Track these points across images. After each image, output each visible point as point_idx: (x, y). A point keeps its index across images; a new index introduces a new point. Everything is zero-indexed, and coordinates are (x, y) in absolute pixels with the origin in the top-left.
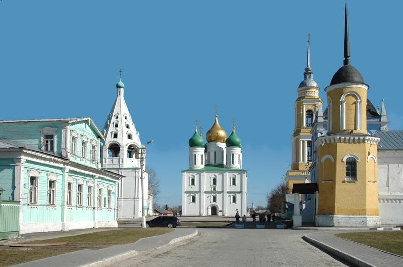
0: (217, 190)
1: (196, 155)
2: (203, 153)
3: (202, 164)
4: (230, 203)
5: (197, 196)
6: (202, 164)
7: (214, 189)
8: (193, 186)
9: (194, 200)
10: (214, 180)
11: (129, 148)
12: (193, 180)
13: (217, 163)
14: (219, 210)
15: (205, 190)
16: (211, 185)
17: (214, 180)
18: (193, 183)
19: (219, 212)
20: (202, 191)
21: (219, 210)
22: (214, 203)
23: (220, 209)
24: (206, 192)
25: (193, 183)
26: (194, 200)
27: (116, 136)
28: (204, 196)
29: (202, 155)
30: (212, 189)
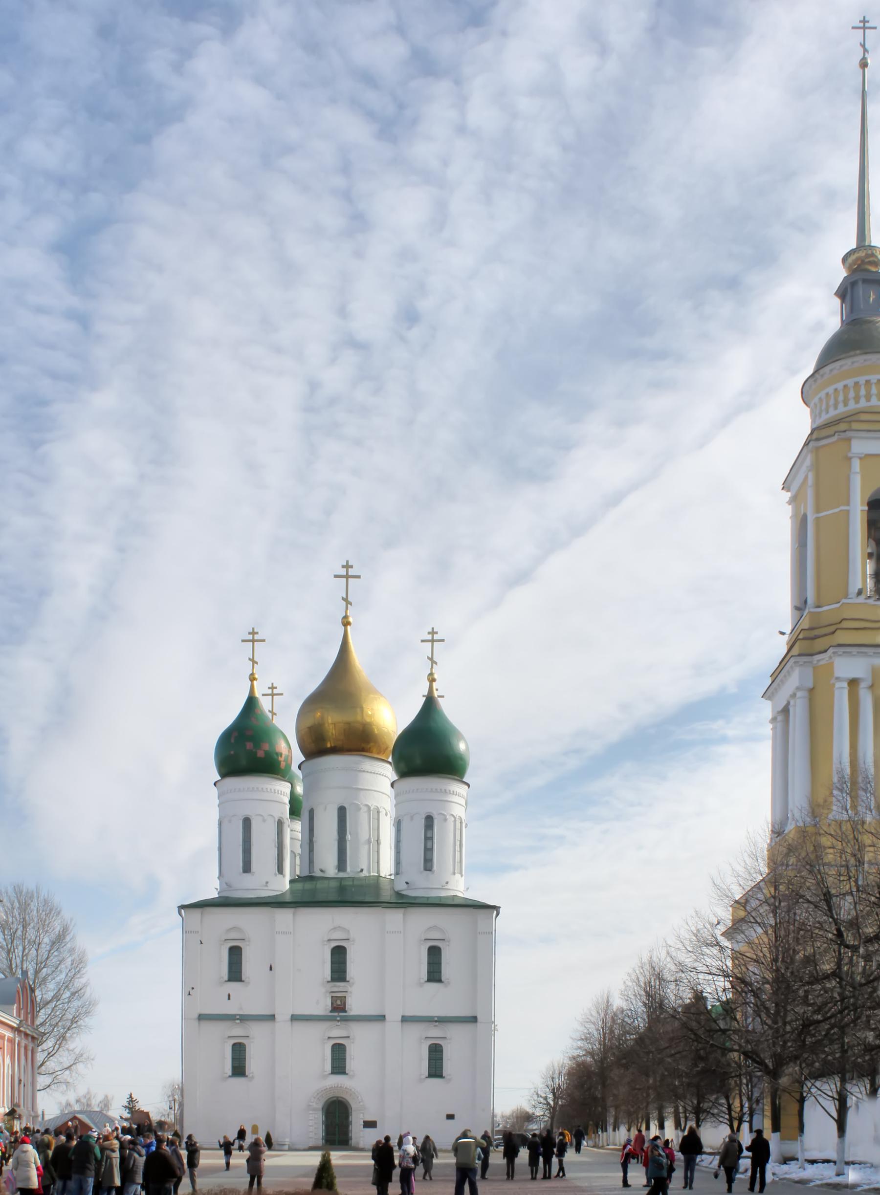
0: (355, 1006)
10: (339, 955)
17: (339, 955)
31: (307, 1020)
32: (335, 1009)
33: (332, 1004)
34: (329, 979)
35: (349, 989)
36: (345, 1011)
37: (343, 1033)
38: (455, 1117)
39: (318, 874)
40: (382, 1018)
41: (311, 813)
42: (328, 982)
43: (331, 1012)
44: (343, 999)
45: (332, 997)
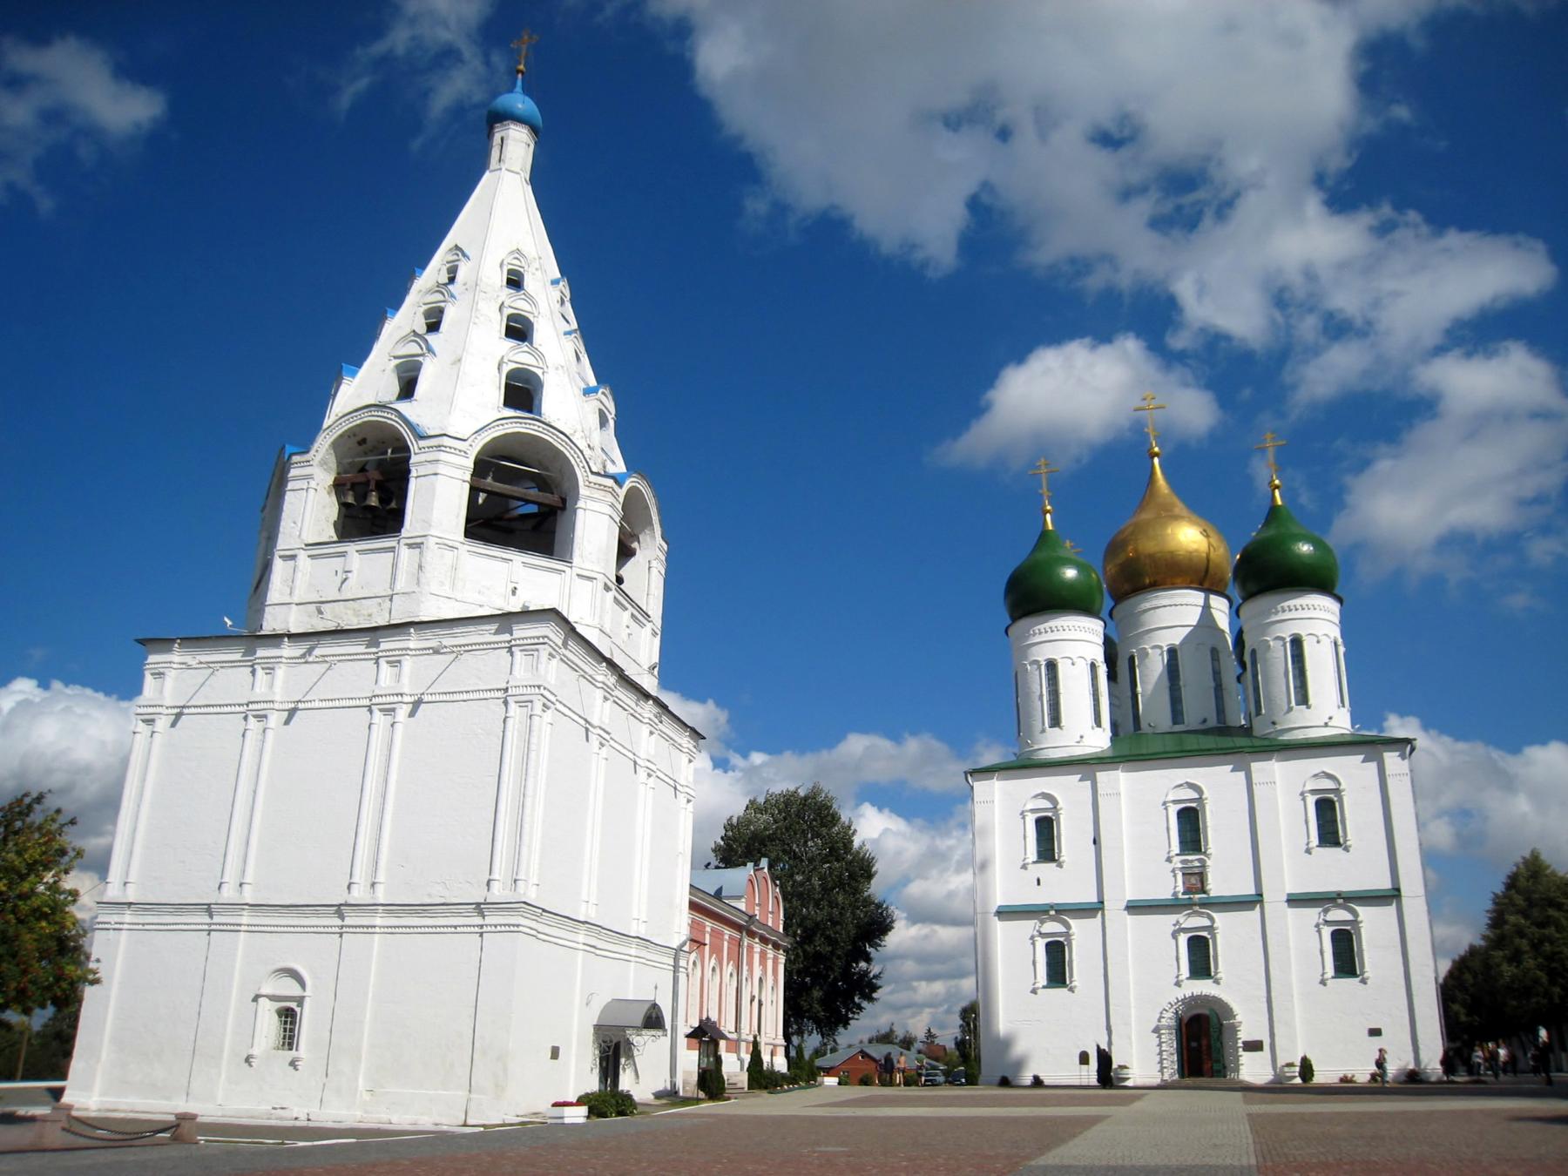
0: (1217, 886)
1: (1052, 666)
2: (1098, 654)
3: (1098, 722)
4: (1323, 982)
5: (1082, 933)
6: (1098, 722)
7: (1196, 879)
8: (1048, 868)
9: (1058, 972)
11: (482, 466)
12: (1046, 829)
13: (1192, 718)
14: (1244, 1035)
15: (1131, 894)
16: (1169, 860)
18: (1047, 849)
19: (1246, 1058)
20: (1114, 906)
21: (1244, 1035)
22: (1203, 987)
23: (1249, 1025)
24: (1135, 908)
25: (1047, 849)
26: (1058, 972)
27: (408, 389)
28: (1131, 932)
29: (1093, 666)
30: (1180, 888)
31: (1150, 906)
32: (1188, 891)
33: (1184, 883)
34: (1178, 852)
35: (1209, 863)
36: (1205, 892)
37: (1206, 922)
38: (1366, 1032)
39: (1150, 731)
40: (1253, 901)
41: (1132, 659)
42: (1177, 855)
43: (1183, 894)
44: (1202, 876)
45: (1183, 874)
